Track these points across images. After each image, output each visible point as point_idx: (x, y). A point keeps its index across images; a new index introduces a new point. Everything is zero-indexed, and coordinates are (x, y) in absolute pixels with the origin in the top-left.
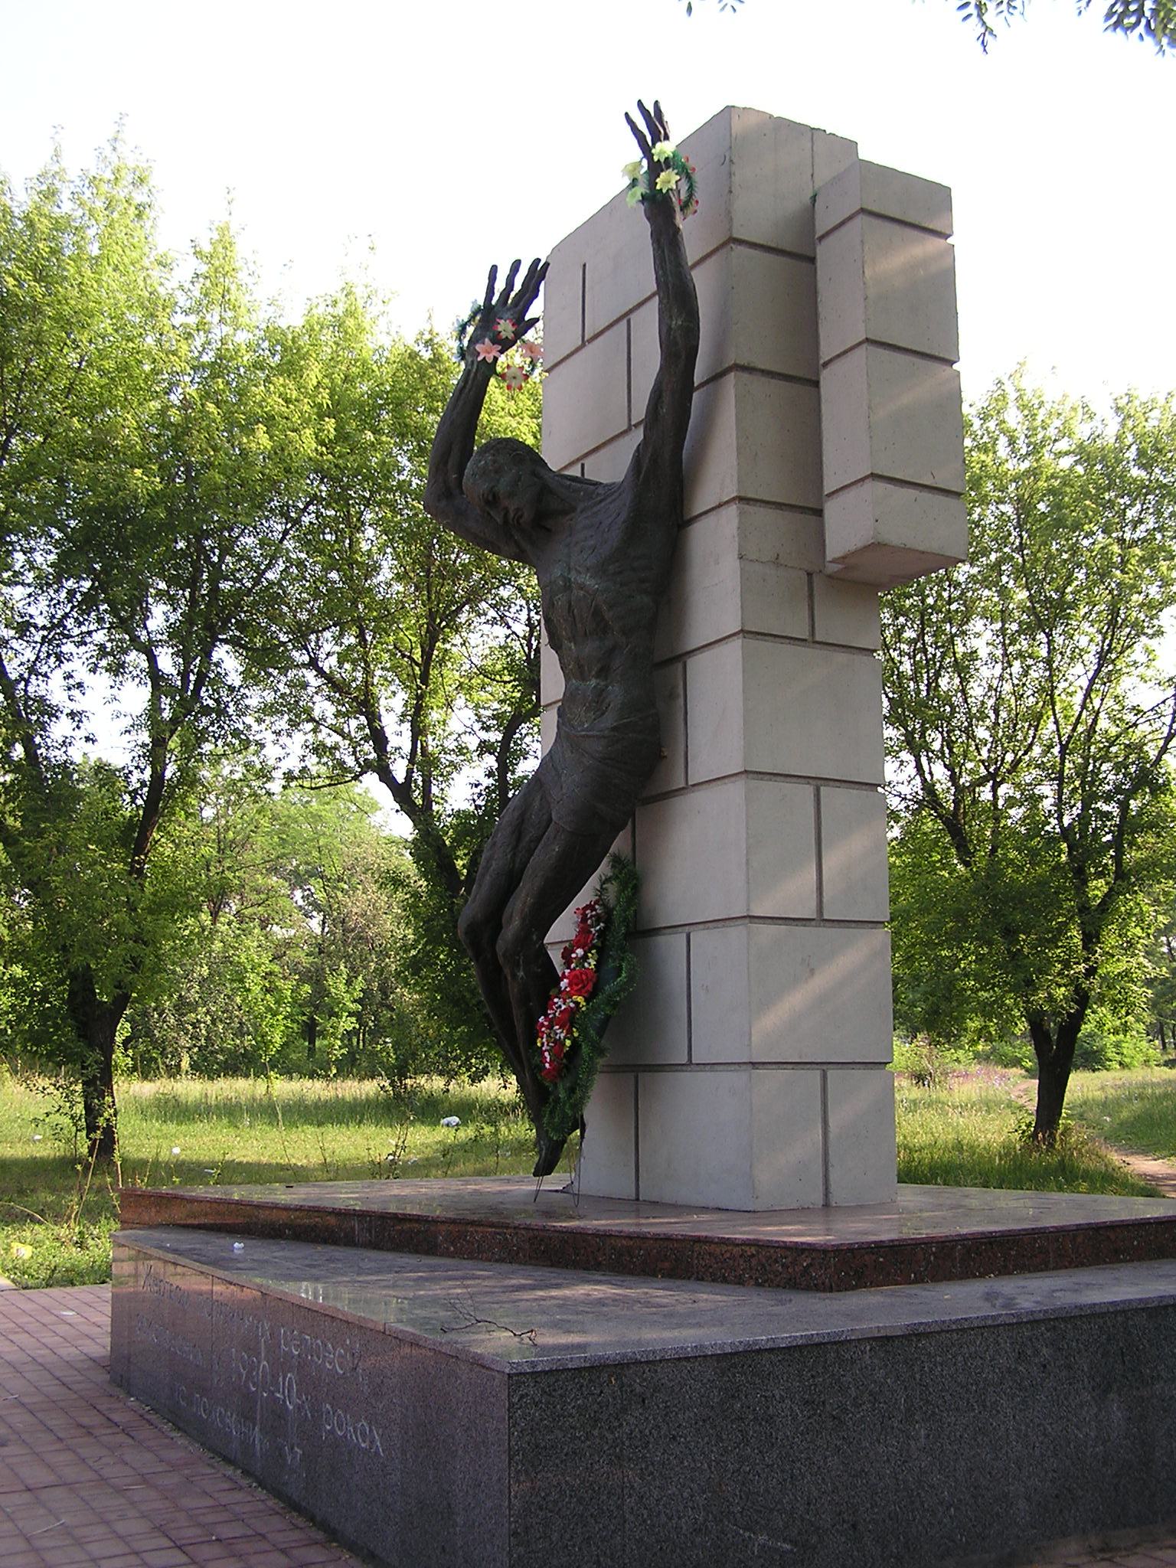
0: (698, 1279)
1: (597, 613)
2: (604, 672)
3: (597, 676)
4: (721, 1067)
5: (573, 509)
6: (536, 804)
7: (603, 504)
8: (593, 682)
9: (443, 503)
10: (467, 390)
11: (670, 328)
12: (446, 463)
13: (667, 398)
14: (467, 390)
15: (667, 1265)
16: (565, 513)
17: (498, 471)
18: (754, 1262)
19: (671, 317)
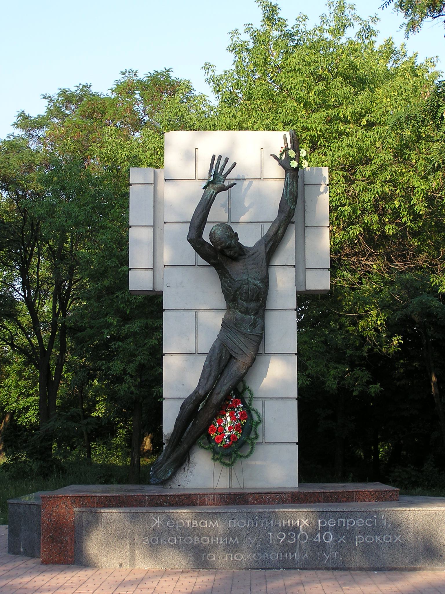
0: (355, 502)
1: (258, 295)
2: (255, 314)
3: (254, 315)
4: (278, 444)
5: (245, 255)
6: (224, 354)
7: (254, 256)
8: (252, 317)
9: (199, 239)
10: (211, 201)
11: (290, 208)
12: (201, 225)
13: (282, 229)
14: (211, 201)
15: (345, 499)
16: (240, 255)
17: (232, 237)
18: (374, 496)
19: (292, 205)
